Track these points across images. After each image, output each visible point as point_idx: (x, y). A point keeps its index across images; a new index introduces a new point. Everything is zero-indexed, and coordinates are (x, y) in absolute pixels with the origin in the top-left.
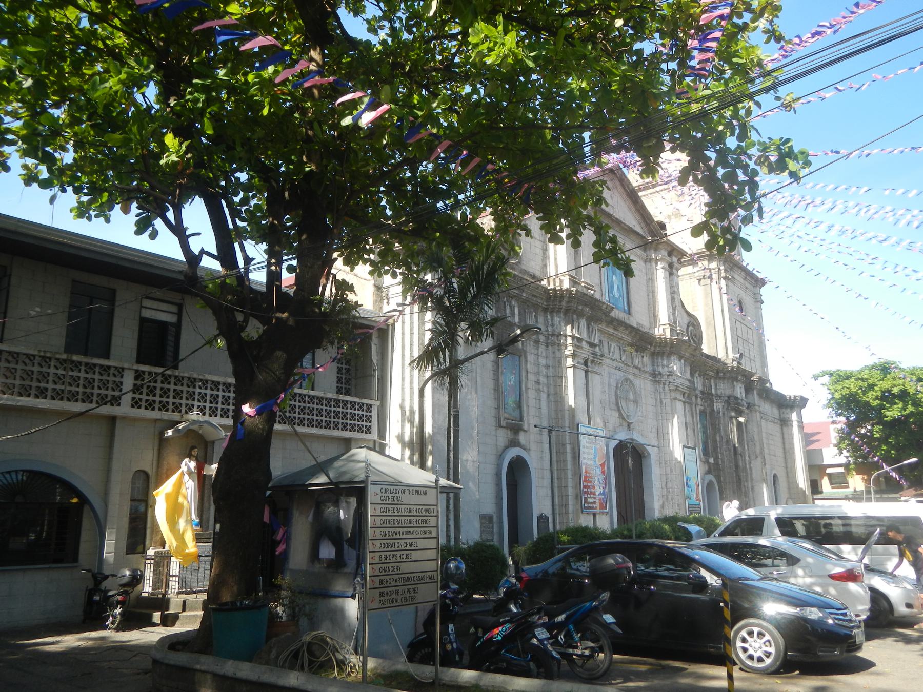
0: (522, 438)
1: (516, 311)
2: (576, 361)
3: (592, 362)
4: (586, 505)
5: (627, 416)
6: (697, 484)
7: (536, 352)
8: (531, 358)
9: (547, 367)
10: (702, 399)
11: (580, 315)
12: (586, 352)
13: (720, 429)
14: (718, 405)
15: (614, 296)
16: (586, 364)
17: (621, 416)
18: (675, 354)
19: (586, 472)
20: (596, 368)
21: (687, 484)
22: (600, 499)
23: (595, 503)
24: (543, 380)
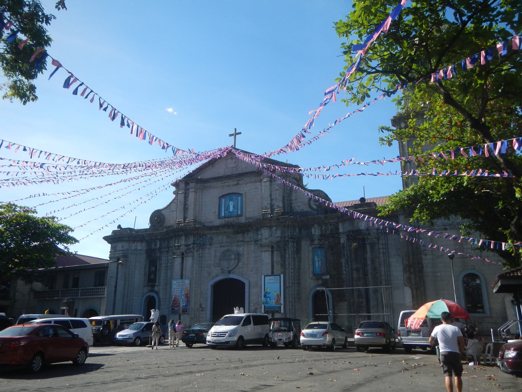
0: (156, 289)
1: (158, 244)
2: (176, 255)
3: (186, 252)
4: (173, 311)
5: (228, 268)
6: (279, 296)
7: (167, 255)
8: (164, 258)
9: (171, 260)
10: (320, 240)
11: (180, 236)
12: (183, 249)
13: (344, 254)
14: (343, 240)
15: (229, 212)
16: (183, 254)
17: (222, 269)
18: (262, 227)
19: (175, 298)
20: (190, 254)
21: (265, 296)
22: (183, 308)
23: (179, 310)
24: (169, 265)
